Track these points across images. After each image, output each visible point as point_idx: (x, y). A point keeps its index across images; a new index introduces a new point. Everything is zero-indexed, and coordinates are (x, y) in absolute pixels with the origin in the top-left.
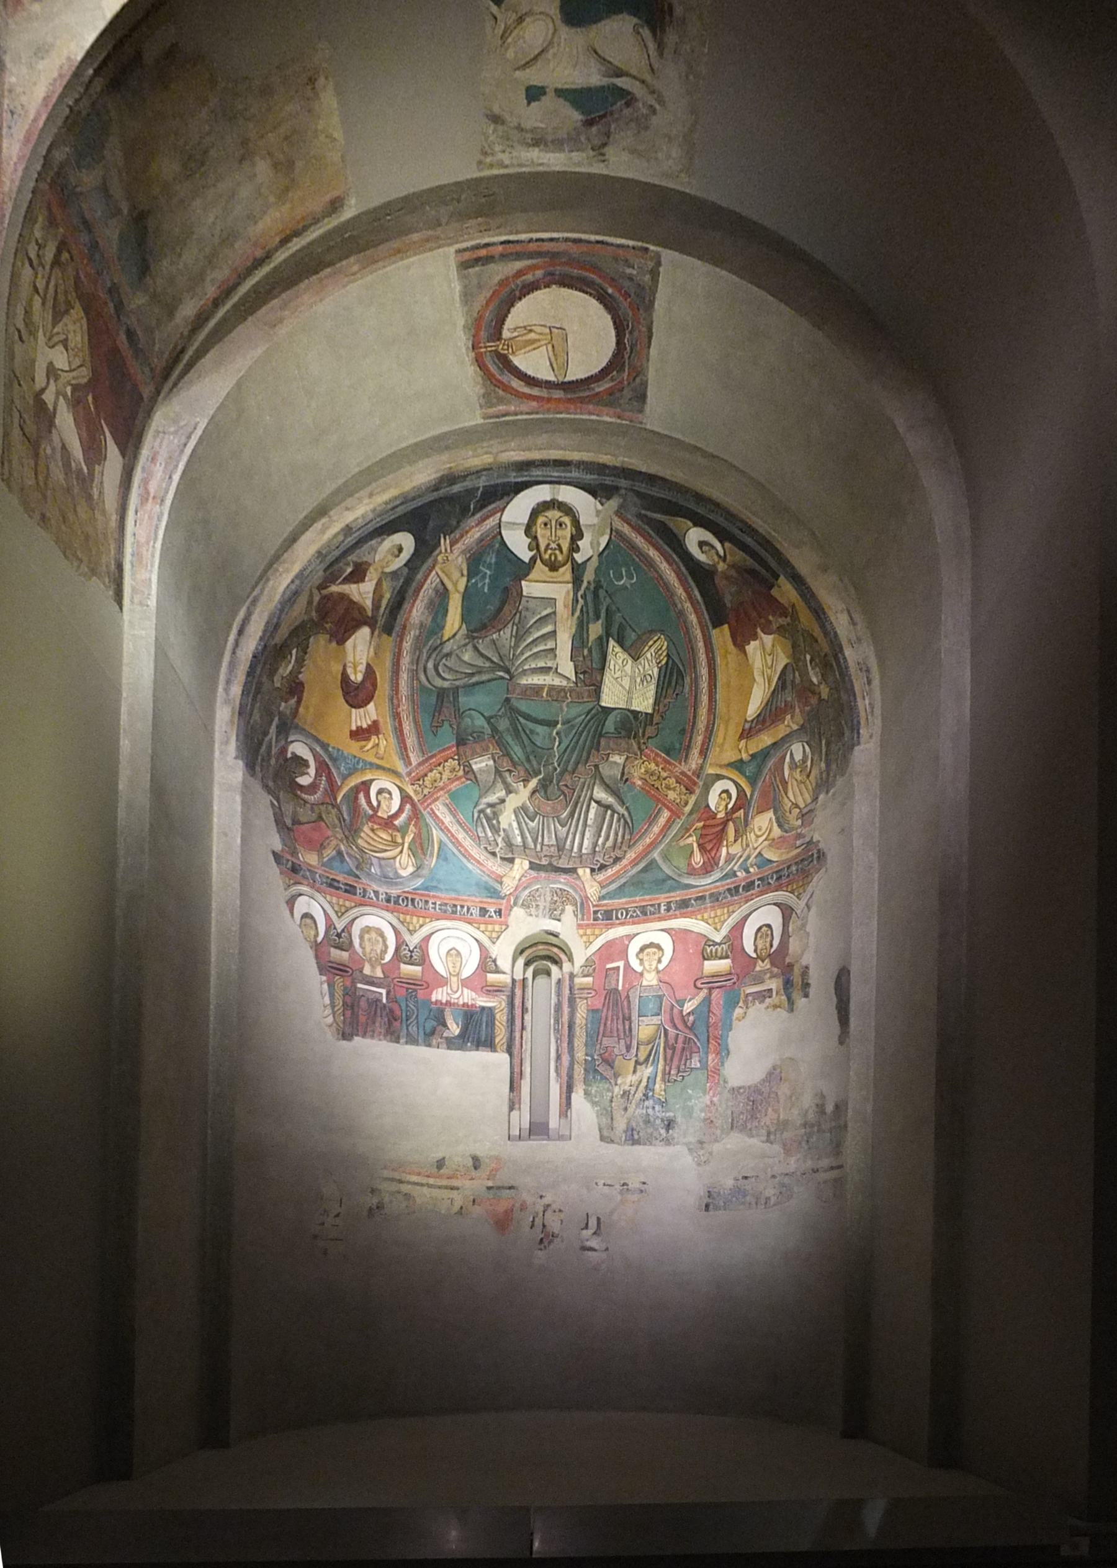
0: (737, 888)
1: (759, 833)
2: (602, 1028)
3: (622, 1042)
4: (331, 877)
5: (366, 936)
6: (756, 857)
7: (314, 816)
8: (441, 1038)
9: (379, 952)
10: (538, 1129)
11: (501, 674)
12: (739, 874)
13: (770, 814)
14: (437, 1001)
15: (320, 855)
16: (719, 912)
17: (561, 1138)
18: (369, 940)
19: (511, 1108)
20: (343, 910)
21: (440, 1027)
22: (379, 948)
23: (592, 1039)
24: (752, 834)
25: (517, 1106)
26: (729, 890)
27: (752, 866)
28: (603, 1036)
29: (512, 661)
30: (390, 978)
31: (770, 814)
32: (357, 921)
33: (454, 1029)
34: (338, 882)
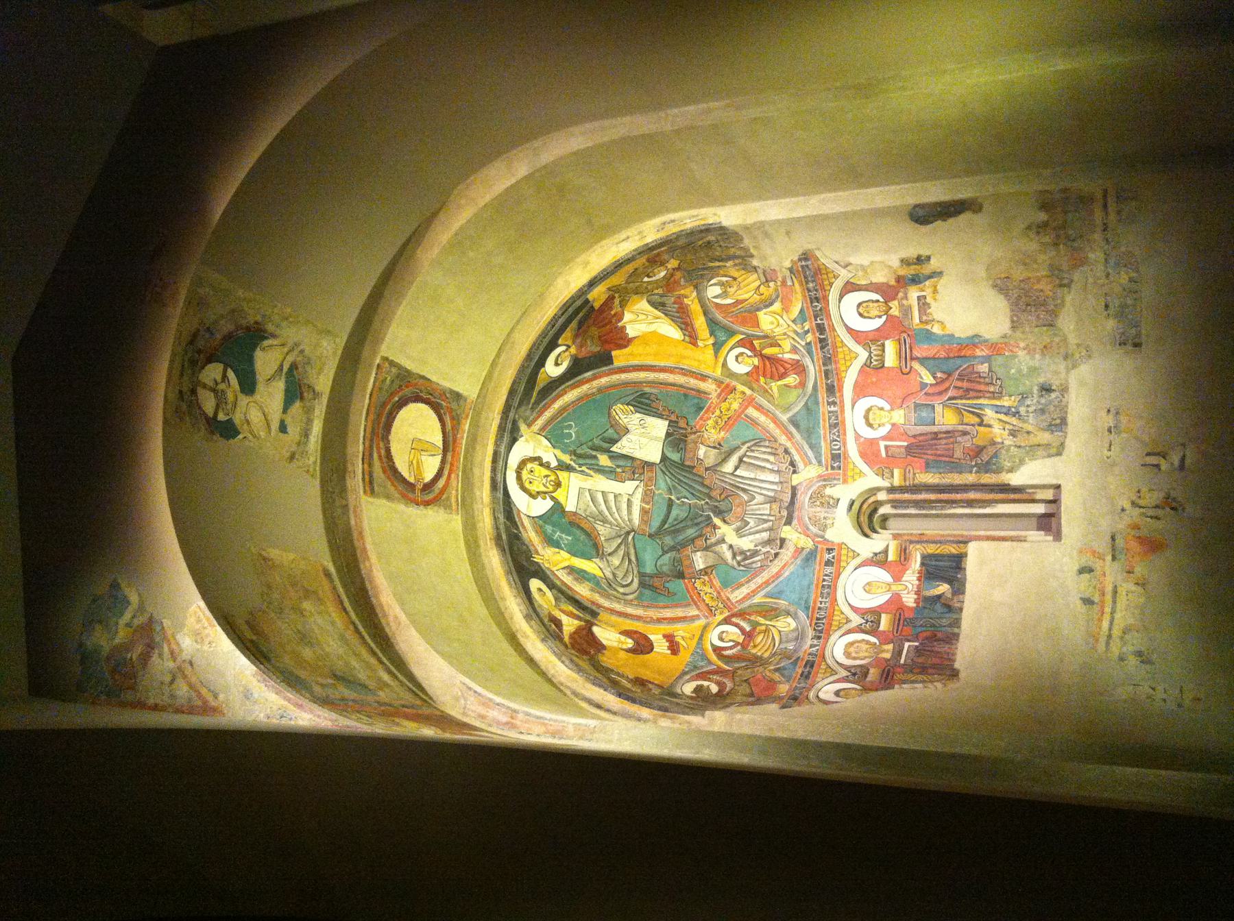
0: (821, 341)
1: (776, 323)
2: (947, 459)
3: (959, 439)
4: (799, 676)
5: (854, 655)
6: (796, 325)
7: (744, 684)
8: (952, 599)
9: (868, 646)
10: (1048, 522)
11: (630, 537)
12: (808, 341)
13: (761, 314)
14: (916, 601)
15: (780, 682)
16: (841, 356)
17: (1055, 501)
18: (856, 653)
19: (1025, 541)
20: (830, 670)
21: (942, 601)
22: (864, 647)
23: (956, 467)
24: (775, 330)
25: (1023, 539)
26: (822, 348)
27: (803, 328)
28: (952, 457)
29: (621, 528)
30: (895, 637)
31: (761, 314)
32: (840, 662)
33: (943, 588)
34: (803, 672)
